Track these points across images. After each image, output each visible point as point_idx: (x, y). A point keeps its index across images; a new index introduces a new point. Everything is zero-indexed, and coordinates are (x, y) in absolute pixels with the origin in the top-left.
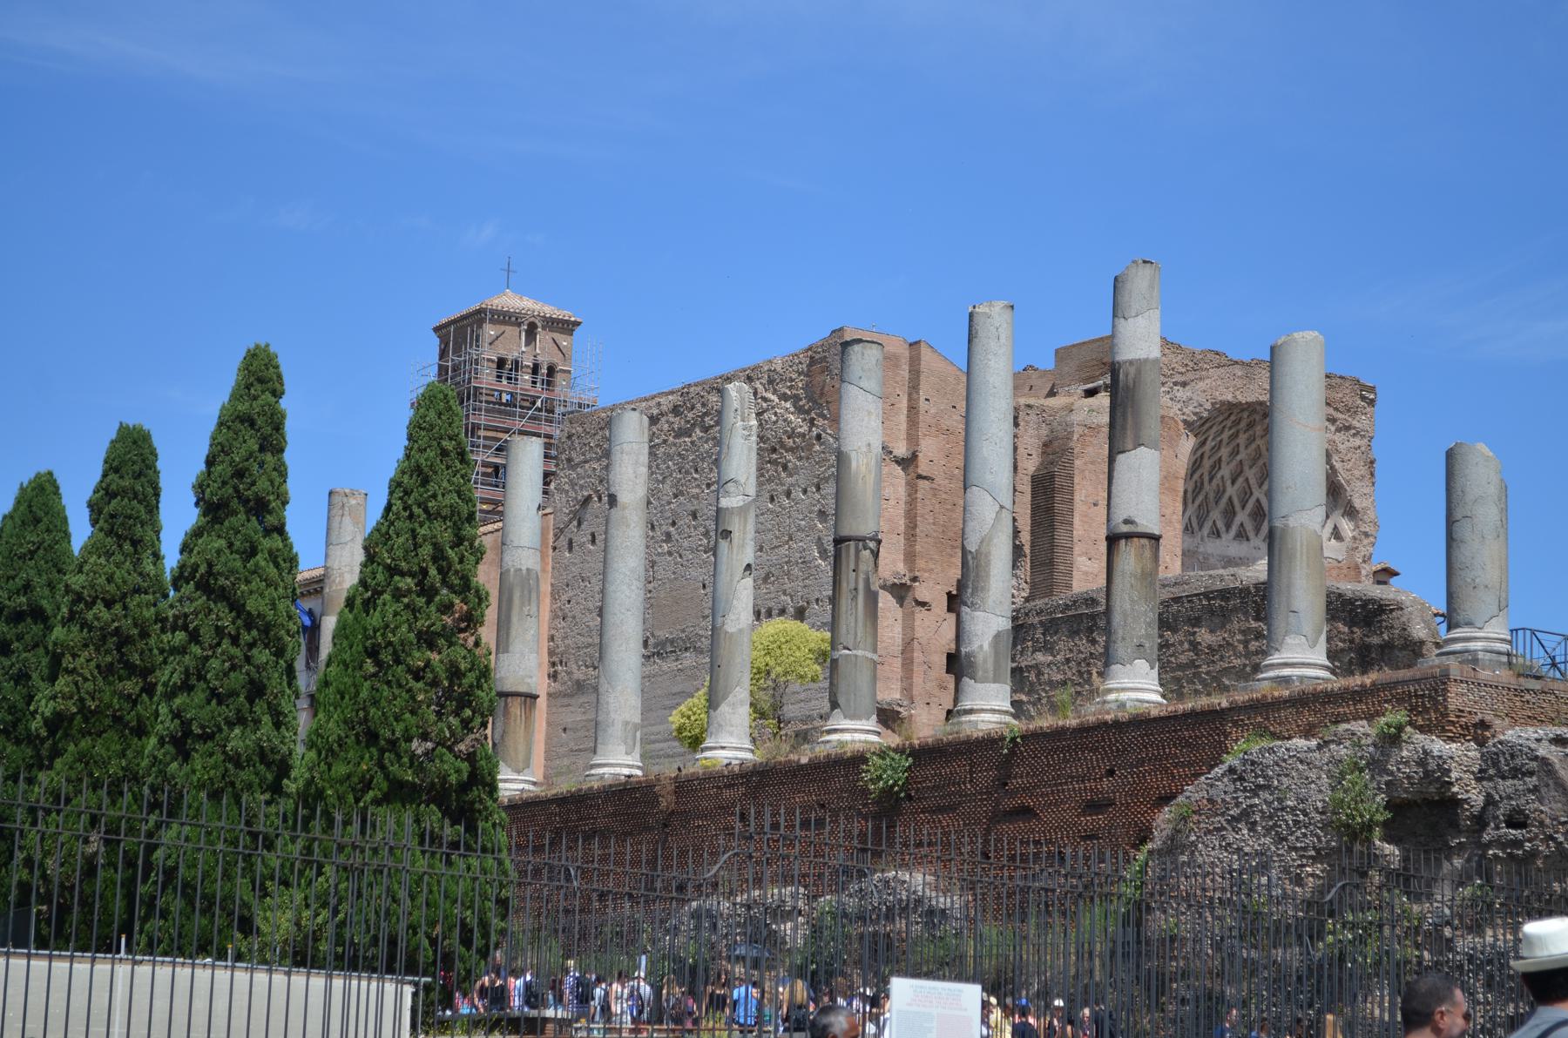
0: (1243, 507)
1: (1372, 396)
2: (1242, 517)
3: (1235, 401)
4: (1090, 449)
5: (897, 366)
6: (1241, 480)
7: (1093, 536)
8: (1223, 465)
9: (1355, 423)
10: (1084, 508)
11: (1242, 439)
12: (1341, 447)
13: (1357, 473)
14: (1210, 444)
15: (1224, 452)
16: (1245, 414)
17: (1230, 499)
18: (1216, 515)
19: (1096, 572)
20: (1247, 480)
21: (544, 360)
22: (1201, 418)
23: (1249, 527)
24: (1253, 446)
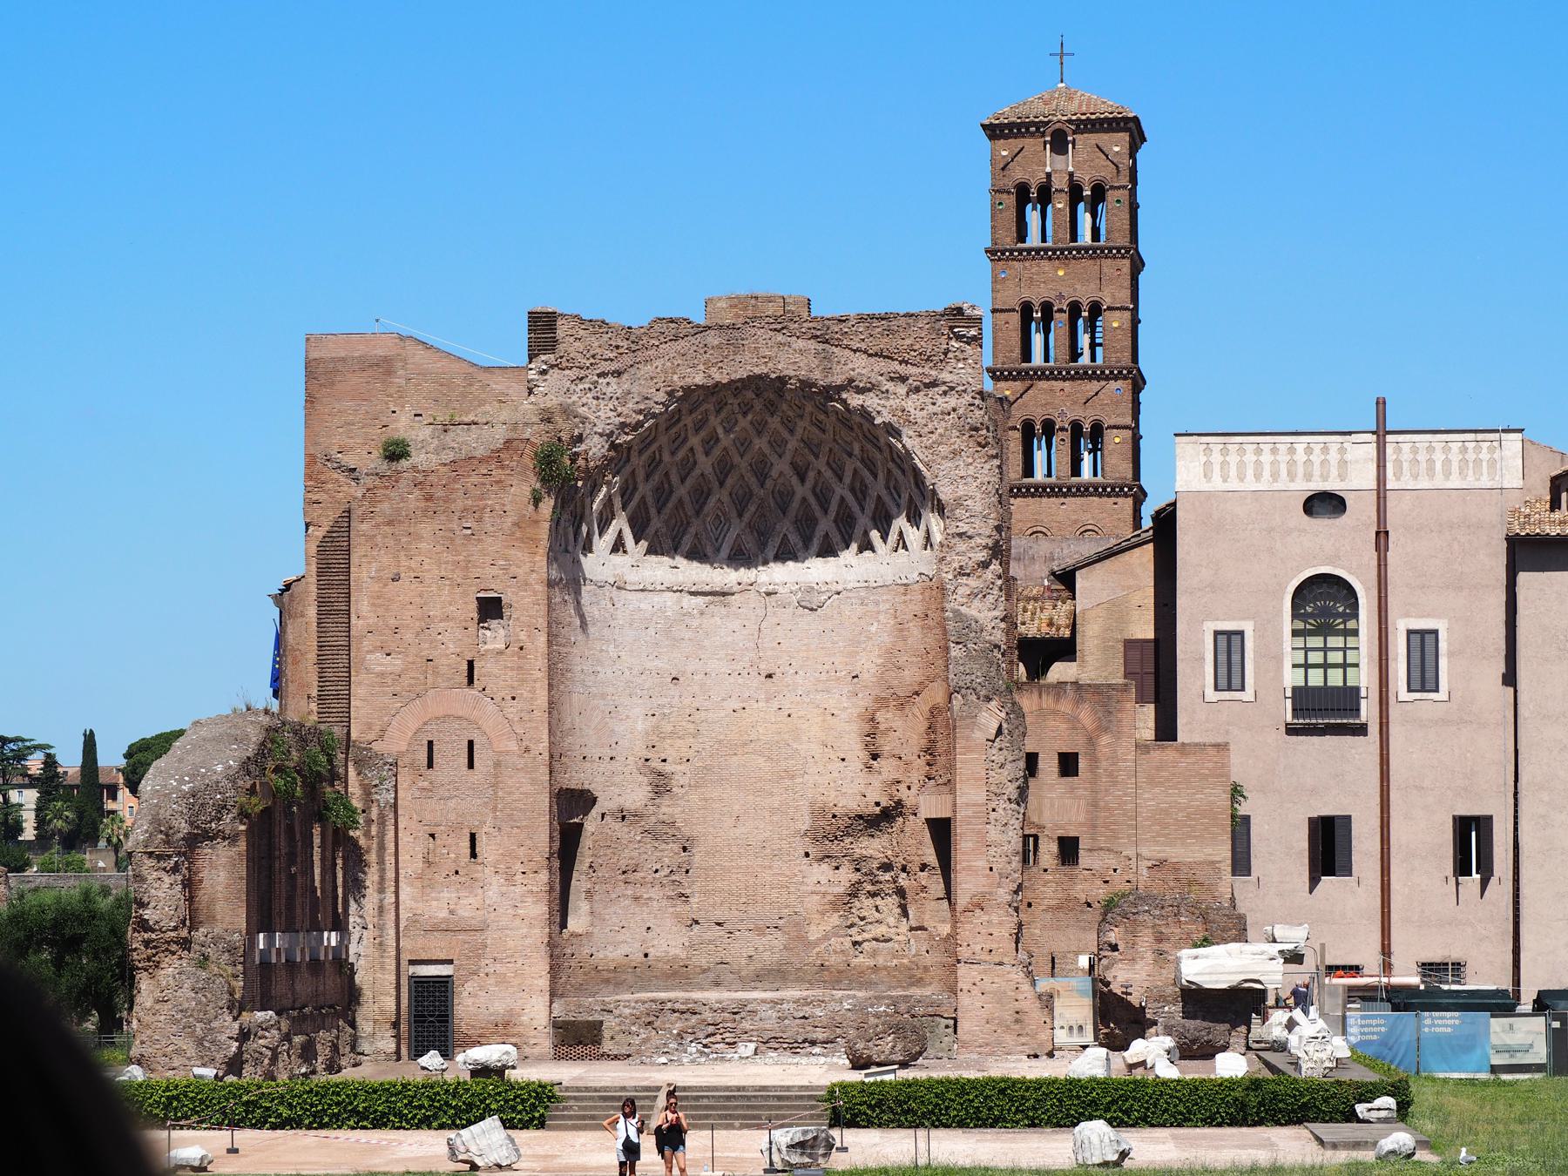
0: (826, 512)
1: (973, 332)
2: (825, 525)
3: (710, 383)
4: (386, 506)
5: (389, 372)
6: (811, 475)
7: (393, 622)
8: (774, 458)
9: (945, 376)
10: (376, 587)
11: (774, 423)
12: (920, 416)
13: (943, 450)
14: (726, 440)
15: (760, 444)
16: (750, 395)
17: (804, 499)
18: (786, 527)
19: (397, 669)
20: (819, 472)
21: (1086, 179)
22: (654, 416)
23: (836, 538)
24: (799, 431)
